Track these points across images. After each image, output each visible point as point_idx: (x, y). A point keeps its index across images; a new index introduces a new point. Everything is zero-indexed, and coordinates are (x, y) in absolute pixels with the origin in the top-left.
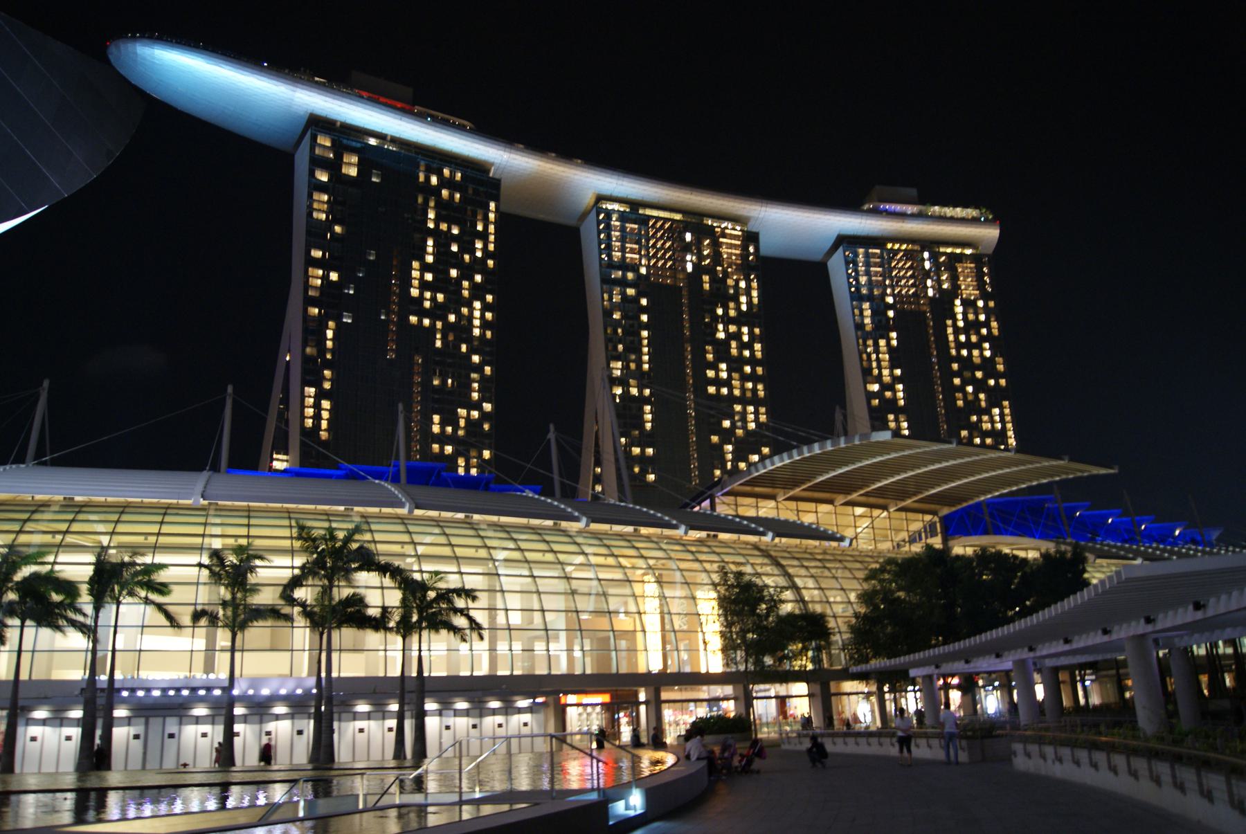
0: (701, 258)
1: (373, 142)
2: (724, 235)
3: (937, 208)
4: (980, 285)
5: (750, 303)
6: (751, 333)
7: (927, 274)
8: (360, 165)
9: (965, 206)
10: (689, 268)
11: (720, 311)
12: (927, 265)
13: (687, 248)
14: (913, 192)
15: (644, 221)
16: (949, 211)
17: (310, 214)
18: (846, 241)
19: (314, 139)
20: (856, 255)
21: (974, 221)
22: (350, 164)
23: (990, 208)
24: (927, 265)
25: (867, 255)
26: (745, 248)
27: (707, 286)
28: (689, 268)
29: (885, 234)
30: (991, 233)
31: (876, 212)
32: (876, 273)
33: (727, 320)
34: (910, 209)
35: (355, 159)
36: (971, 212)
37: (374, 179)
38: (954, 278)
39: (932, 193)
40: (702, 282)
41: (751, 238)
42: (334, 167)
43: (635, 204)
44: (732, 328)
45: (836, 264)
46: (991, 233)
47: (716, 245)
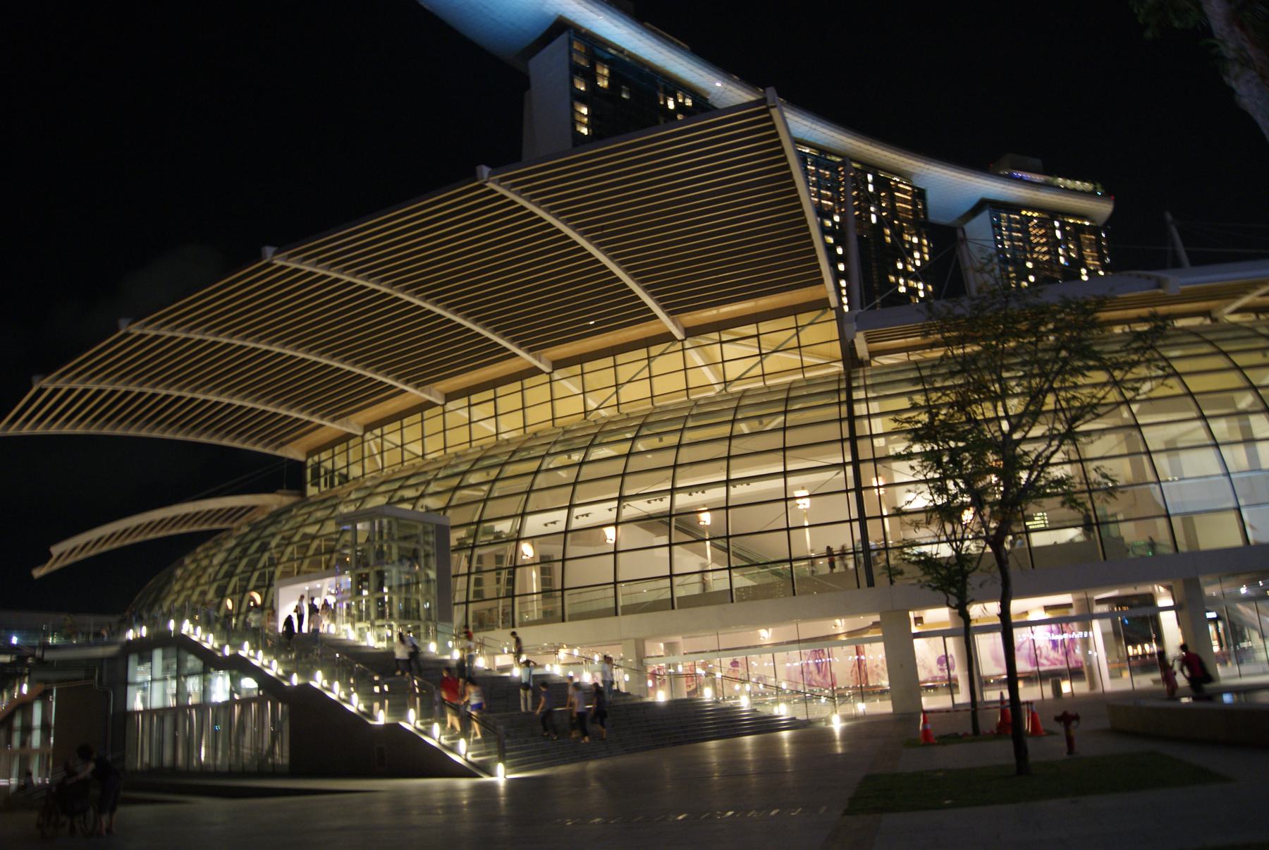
0: (880, 209)
1: (612, 51)
2: (900, 190)
3: (1060, 180)
4: (1101, 258)
5: (922, 259)
6: (925, 290)
7: (1058, 243)
8: (611, 78)
9: (1083, 180)
10: (874, 219)
11: (900, 266)
12: (1058, 234)
13: (874, 199)
14: (1038, 162)
15: (832, 167)
16: (1069, 183)
17: (574, 127)
18: (984, 204)
19: (570, 44)
20: (999, 219)
21: (1091, 194)
22: (603, 76)
23: (1104, 187)
24: (1058, 234)
25: (1010, 220)
26: (914, 204)
27: (888, 239)
28: (874, 219)
29: (1020, 201)
30: (1103, 208)
31: (1011, 178)
32: (1019, 240)
33: (906, 274)
34: (1038, 178)
35: (606, 72)
36: (1088, 186)
37: (624, 96)
38: (1080, 250)
39: (1055, 164)
40: (884, 234)
41: (920, 194)
42: (591, 77)
43: (823, 151)
44: (911, 283)
45: (979, 227)
46: (1103, 208)
47: (893, 199)
